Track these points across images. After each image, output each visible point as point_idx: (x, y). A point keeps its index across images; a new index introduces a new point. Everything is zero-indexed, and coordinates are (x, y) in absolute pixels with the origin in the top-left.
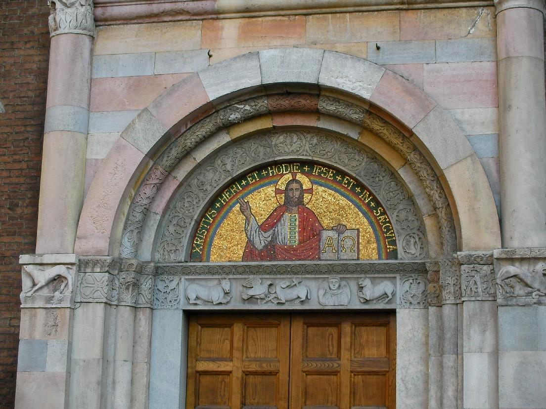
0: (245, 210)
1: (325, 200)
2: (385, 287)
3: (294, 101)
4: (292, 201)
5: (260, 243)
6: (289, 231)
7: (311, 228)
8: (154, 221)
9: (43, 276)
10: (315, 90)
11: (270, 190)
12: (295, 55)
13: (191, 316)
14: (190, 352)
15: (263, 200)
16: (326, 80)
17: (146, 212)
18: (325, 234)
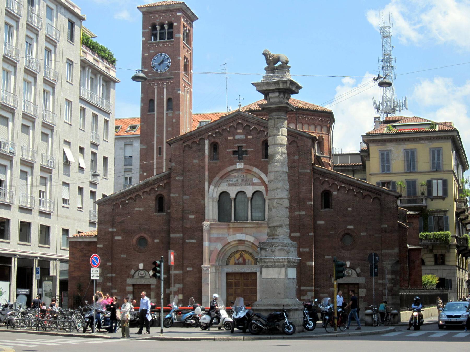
0: (234, 257)
1: (247, 256)
2: (255, 269)
3: (241, 242)
4: (241, 256)
5: (237, 262)
6: (241, 260)
7: (244, 260)
8: (221, 260)
9: (205, 269)
10: (244, 241)
11: (238, 254)
12: (242, 235)
13: (227, 274)
14: (227, 279)
15: (237, 256)
16: (246, 239)
17: (220, 258)
18: (247, 261)
